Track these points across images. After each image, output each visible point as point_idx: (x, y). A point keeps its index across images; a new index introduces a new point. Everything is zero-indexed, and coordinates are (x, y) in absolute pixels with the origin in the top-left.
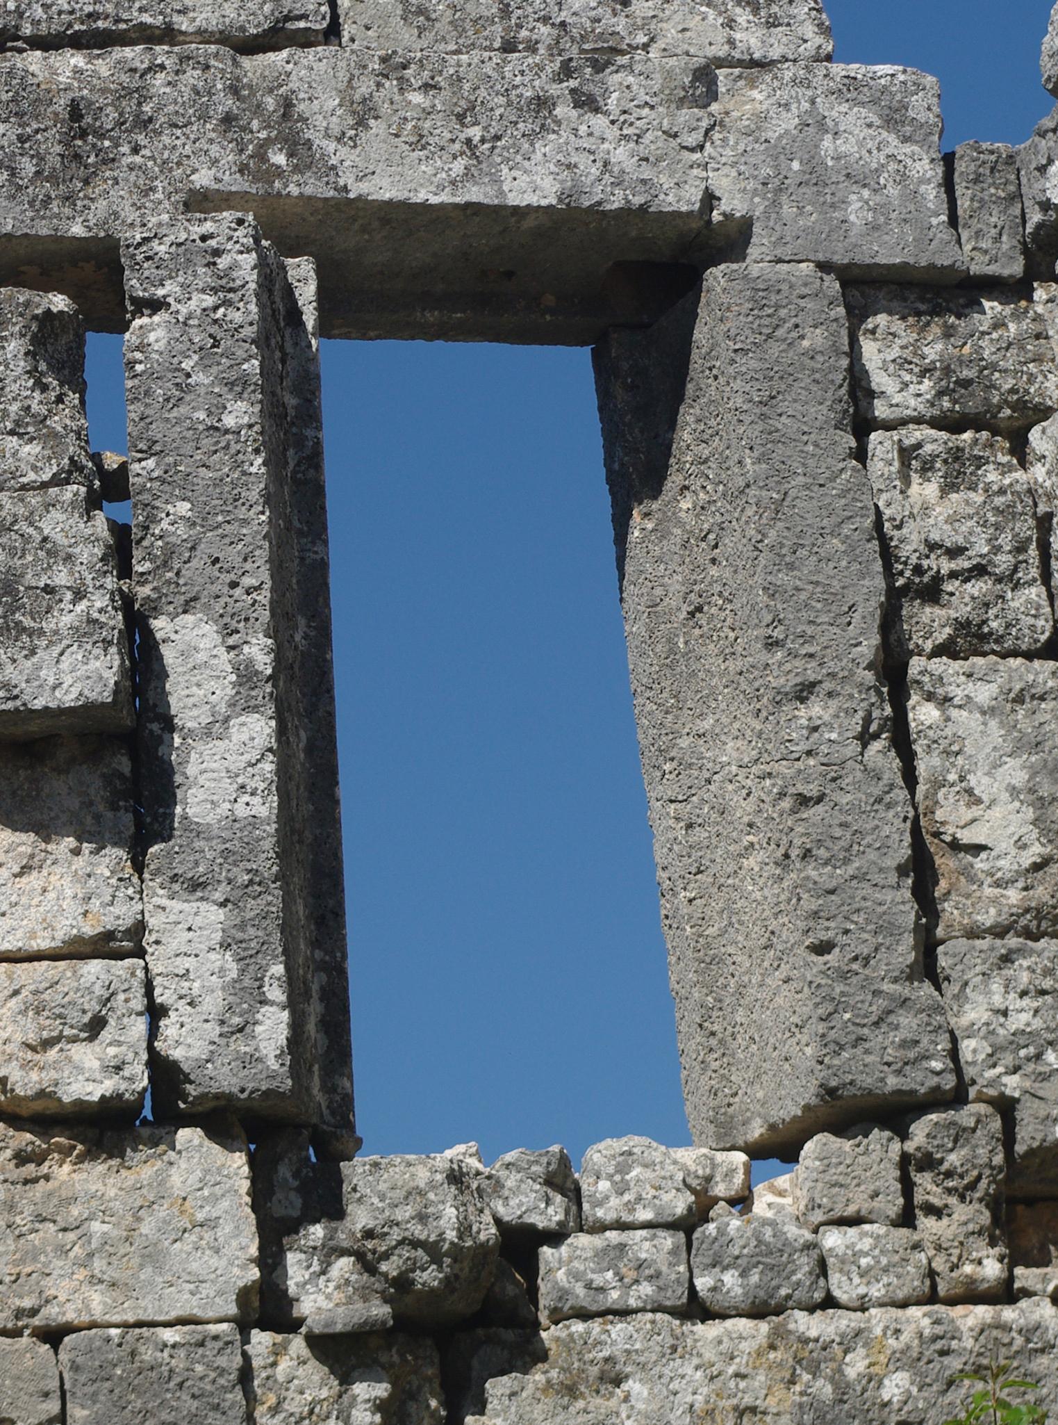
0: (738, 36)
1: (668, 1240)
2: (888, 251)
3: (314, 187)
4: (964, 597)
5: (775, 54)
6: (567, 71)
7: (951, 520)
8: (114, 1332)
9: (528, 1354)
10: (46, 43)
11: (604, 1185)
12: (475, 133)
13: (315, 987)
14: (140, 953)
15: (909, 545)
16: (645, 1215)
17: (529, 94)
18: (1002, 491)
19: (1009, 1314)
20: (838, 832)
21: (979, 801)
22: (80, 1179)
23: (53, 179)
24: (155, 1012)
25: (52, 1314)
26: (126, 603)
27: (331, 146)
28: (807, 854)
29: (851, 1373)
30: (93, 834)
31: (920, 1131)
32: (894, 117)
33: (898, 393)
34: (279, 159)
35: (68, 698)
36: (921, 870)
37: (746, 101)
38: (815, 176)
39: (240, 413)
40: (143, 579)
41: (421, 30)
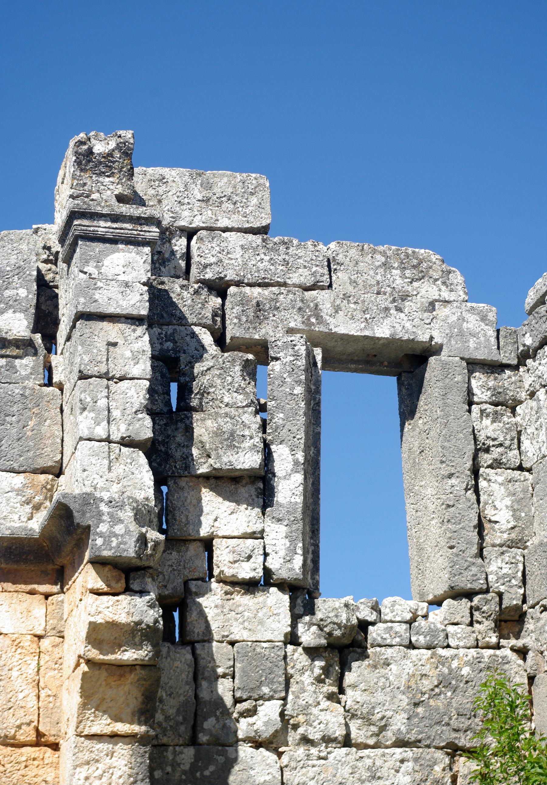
0: (441, 293)
1: (404, 626)
2: (480, 355)
3: (322, 329)
4: (496, 452)
5: (452, 299)
7: (494, 431)
8: (249, 643)
9: (364, 656)
12: (368, 316)
13: (310, 550)
15: (482, 437)
16: (398, 619)
17: (383, 306)
18: (508, 423)
19: (498, 652)
20: (458, 515)
21: (497, 509)
22: (242, 600)
23: (251, 322)
24: (266, 555)
25: (233, 637)
26: (264, 441)
27: (328, 318)
28: (449, 521)
29: (453, 666)
30: (251, 504)
31: (476, 600)
32: (484, 319)
33: (481, 394)
34: (313, 320)
35: (247, 466)
36: (480, 527)
37: (442, 312)
38: (461, 333)
39: (299, 390)
40: (269, 434)
41: (355, 287)
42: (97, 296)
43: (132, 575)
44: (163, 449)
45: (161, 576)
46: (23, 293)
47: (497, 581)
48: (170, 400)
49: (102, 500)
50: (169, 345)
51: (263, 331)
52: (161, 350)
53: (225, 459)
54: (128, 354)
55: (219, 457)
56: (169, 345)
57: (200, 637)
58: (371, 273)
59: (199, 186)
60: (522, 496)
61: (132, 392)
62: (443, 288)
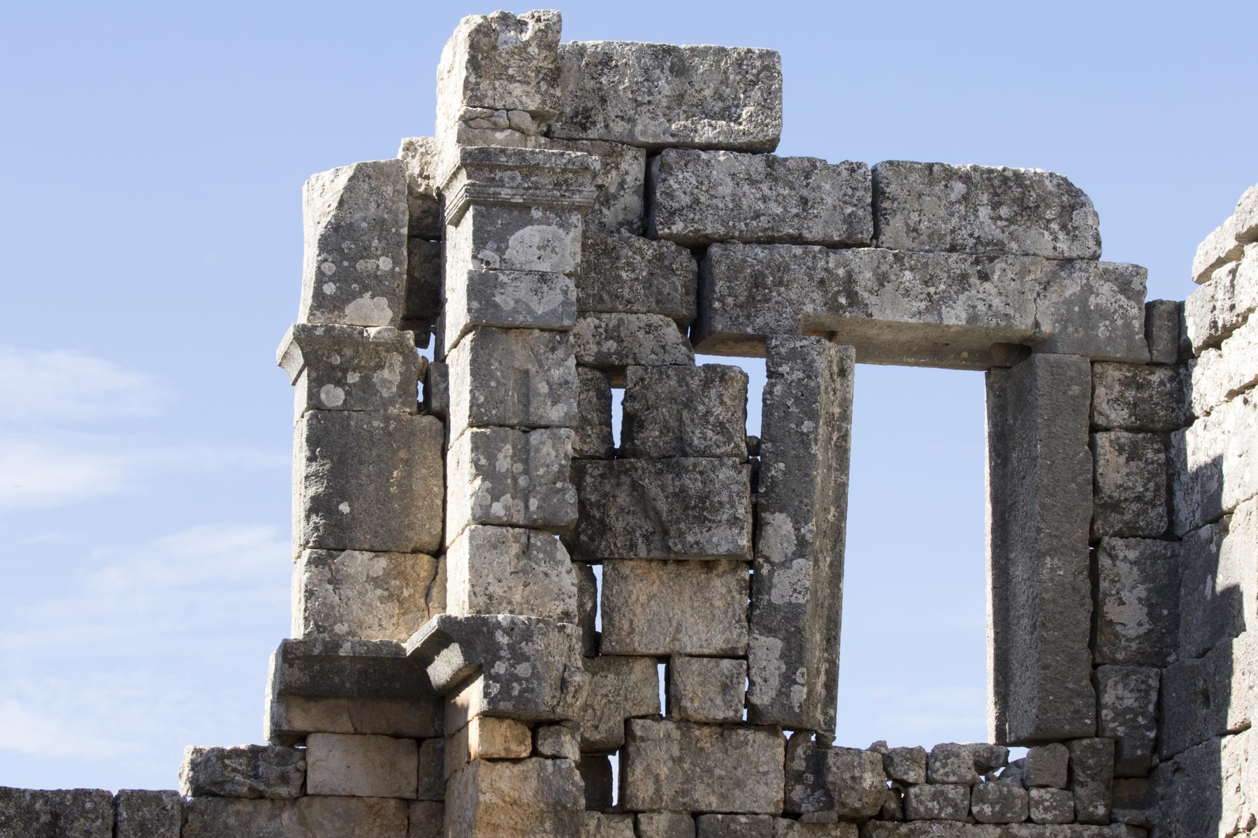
0: (1058, 245)
1: (961, 790)
5: (1075, 256)
6: (977, 262)
7: (1128, 474)
8: (720, 816)
10: (746, 242)
11: (938, 764)
12: (932, 290)
13: (823, 670)
14: (745, 657)
16: (952, 779)
17: (958, 272)
18: (1153, 463)
19: (1106, 830)
20: (1058, 616)
23: (741, 306)
27: (866, 295)
28: (1043, 625)
34: (843, 300)
41: (914, 239)
42: (498, 299)
43: (541, 731)
44: (598, 516)
45: (590, 711)
46: (385, 264)
47: (1113, 720)
48: (610, 434)
49: (498, 625)
50: (611, 345)
51: (759, 321)
52: (599, 353)
53: (690, 539)
54: (543, 388)
55: (681, 534)
56: (611, 345)
57: (647, 806)
58: (942, 212)
59: (667, 72)
60: (1165, 581)
61: (547, 449)
62: (1061, 235)
